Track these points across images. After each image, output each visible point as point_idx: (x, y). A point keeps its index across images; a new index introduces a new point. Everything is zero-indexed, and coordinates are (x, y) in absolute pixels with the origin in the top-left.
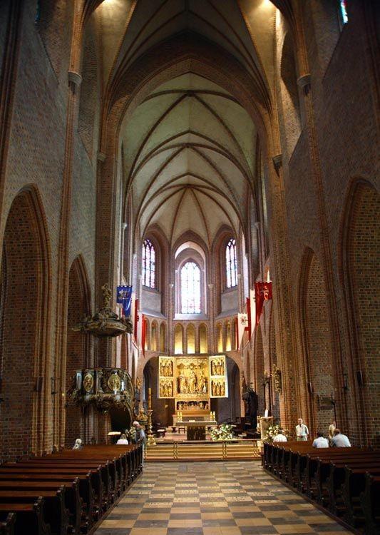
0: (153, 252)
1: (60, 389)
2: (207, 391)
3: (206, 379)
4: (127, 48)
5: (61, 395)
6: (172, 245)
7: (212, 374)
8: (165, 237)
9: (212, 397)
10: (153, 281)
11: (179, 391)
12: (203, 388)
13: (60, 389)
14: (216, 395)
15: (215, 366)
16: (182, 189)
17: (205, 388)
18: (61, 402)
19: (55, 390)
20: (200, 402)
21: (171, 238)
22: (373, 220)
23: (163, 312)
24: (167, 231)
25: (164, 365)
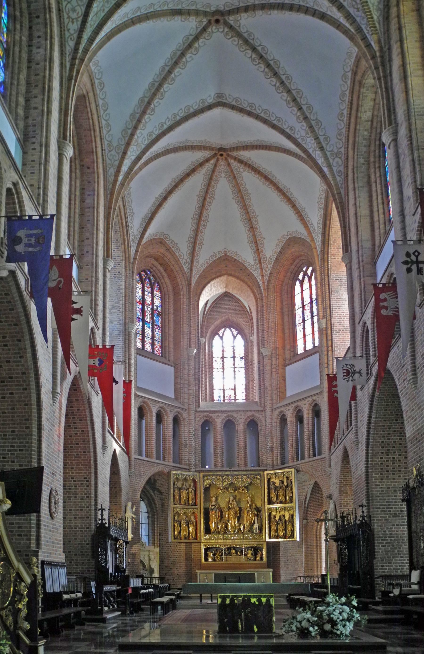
0: (157, 294)
3: (259, 511)
7: (270, 502)
8: (181, 267)
9: (268, 540)
10: (157, 344)
14: (278, 537)
15: (276, 488)
16: (207, 160)
17: (256, 526)
23: (177, 398)
24: (183, 250)
25: (179, 485)
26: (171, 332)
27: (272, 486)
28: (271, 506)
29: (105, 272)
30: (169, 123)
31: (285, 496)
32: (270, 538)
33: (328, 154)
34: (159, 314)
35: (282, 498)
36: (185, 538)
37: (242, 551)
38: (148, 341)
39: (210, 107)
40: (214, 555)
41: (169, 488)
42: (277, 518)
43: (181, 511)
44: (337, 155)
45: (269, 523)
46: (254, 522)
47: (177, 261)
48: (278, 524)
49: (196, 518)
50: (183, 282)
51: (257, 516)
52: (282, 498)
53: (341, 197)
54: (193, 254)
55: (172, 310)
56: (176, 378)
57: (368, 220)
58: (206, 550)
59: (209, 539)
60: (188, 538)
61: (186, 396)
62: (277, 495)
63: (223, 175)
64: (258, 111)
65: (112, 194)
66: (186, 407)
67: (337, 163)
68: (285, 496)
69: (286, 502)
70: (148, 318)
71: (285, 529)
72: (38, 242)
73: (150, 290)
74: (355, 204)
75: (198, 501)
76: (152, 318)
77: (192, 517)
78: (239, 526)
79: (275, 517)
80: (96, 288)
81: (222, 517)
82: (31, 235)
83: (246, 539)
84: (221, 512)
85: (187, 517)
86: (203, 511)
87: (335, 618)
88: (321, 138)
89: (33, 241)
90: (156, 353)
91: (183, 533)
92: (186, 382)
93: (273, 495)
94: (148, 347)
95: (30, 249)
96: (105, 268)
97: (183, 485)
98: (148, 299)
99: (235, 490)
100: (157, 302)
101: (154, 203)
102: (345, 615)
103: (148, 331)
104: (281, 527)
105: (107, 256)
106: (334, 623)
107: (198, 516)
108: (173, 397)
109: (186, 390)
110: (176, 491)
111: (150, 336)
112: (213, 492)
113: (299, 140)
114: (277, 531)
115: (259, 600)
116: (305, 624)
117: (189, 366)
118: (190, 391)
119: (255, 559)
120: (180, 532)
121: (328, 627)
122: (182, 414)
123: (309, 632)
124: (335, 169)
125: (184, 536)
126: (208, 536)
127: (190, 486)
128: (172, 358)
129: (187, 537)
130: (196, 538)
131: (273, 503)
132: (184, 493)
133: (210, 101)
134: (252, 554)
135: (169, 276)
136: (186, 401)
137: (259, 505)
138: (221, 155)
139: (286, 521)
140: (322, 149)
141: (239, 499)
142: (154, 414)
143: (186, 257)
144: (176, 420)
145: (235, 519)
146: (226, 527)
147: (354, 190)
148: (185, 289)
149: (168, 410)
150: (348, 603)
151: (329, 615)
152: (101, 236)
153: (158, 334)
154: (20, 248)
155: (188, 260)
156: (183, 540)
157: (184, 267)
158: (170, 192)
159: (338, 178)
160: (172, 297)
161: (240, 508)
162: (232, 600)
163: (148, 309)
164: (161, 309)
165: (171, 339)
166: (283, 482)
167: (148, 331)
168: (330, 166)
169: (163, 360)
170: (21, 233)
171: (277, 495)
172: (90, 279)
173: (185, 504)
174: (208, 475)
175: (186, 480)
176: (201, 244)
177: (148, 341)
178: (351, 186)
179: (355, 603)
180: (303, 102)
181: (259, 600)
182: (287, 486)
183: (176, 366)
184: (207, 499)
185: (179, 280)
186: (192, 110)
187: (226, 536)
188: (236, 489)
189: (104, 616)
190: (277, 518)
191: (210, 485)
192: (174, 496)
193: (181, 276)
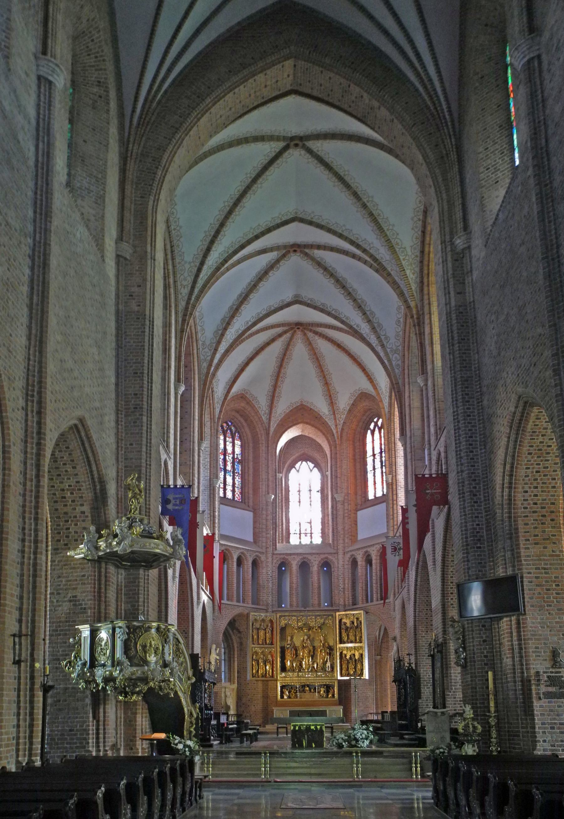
0: (238, 443)
1: (32, 655)
3: (331, 650)
5: (32, 667)
6: (272, 429)
7: (341, 642)
9: (339, 678)
11: (284, 669)
12: (325, 663)
13: (32, 655)
15: (347, 629)
16: (285, 332)
17: (328, 664)
18: (32, 678)
19: (20, 655)
20: (321, 686)
21: (270, 419)
23: (255, 542)
24: (262, 403)
26: (251, 478)
27: (343, 627)
28: (342, 645)
29: (199, 452)
30: (253, 321)
31: (355, 636)
32: (341, 676)
33: (388, 350)
34: (240, 462)
35: (352, 638)
36: (263, 676)
38: (229, 488)
39: (288, 305)
40: (289, 692)
41: (247, 628)
42: (348, 657)
43: (260, 651)
44: (396, 352)
46: (327, 661)
47: (257, 412)
48: (348, 663)
49: (272, 656)
50: (262, 432)
52: (352, 638)
53: (399, 387)
54: (271, 406)
55: (251, 458)
56: (255, 522)
57: (420, 411)
58: (282, 687)
59: (285, 677)
60: (265, 676)
61: (264, 539)
62: (348, 635)
63: (300, 341)
64: (329, 309)
65: (205, 384)
66: (264, 551)
67: (396, 358)
68: (355, 636)
69: (355, 642)
70: (229, 468)
71: (355, 668)
72: (181, 503)
73: (231, 440)
74: (410, 397)
75: (275, 640)
76: (233, 467)
77: (269, 656)
78: (313, 664)
79: (346, 656)
80: (193, 470)
81: (297, 656)
82: (177, 498)
83: (319, 676)
84: (296, 650)
85: (264, 655)
86: (279, 650)
87: (357, 737)
88: (383, 338)
89: (178, 503)
90: (236, 499)
91: (260, 672)
92: (264, 527)
93: (344, 635)
94: (229, 495)
95: (177, 508)
96: (199, 449)
97: (261, 625)
98: (229, 449)
99: (309, 630)
100: (238, 450)
101: (237, 369)
102: (364, 736)
103: (229, 480)
104: (351, 666)
105: (201, 439)
106: (357, 740)
107: (275, 655)
108: (252, 540)
109: (264, 534)
110: (255, 631)
111: (231, 484)
112: (288, 631)
113: (365, 335)
114: (348, 669)
116: (340, 741)
117: (267, 511)
118: (268, 535)
119: (327, 697)
120: (258, 671)
121: (354, 743)
122: (260, 558)
123: (343, 746)
124: (394, 363)
125: (262, 674)
126: (283, 674)
127: (267, 626)
128: (251, 504)
129: (264, 675)
130: (273, 676)
131: (344, 643)
132: (262, 633)
133: (289, 300)
135: (249, 426)
136: (264, 544)
137: (331, 644)
138: (298, 328)
139: (356, 660)
140: (383, 346)
141: (313, 638)
142: (235, 560)
143: (264, 409)
144: (255, 563)
145: (308, 657)
146: (301, 665)
147: (409, 384)
148: (263, 438)
149: (248, 555)
150: (367, 729)
151: (354, 736)
152: (196, 423)
153: (238, 480)
154: (170, 507)
155: (267, 411)
156: (260, 678)
157: (263, 418)
158: (251, 359)
159: (397, 371)
160: (251, 445)
161: (314, 647)
162: (300, 727)
163: (229, 458)
164: (242, 457)
165: (251, 486)
166: (353, 623)
167: (229, 480)
168: (389, 360)
169: (243, 505)
170: (170, 497)
171: (348, 635)
172: (188, 463)
173: (263, 644)
174: (284, 616)
175: (263, 620)
176: (279, 397)
177: (229, 488)
178: (406, 380)
179: (371, 729)
180: (367, 309)
182: (357, 627)
183: (255, 511)
184: (283, 637)
185: (258, 430)
186: (273, 308)
187: (300, 674)
188: (310, 628)
189: (212, 742)
190: (348, 657)
191: (286, 625)
192: (253, 636)
193: (260, 426)
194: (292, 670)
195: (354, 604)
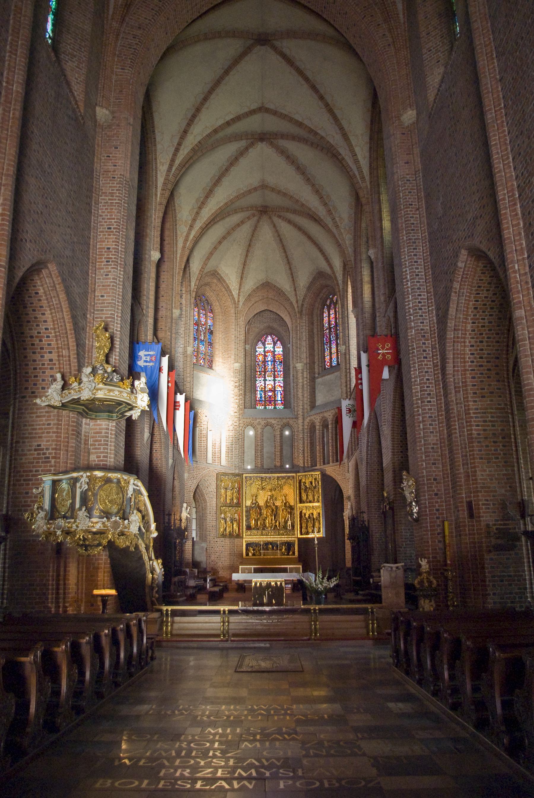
2: (293, 526)
4: (159, 239)
7: (301, 501)
9: (299, 536)
11: (249, 528)
12: (286, 522)
17: (289, 523)
22: (467, 340)
27: (303, 487)
32: (301, 534)
37: (277, 546)
42: (307, 516)
45: (300, 521)
51: (290, 513)
52: (311, 498)
58: (248, 545)
62: (307, 496)
78: (276, 522)
79: (305, 515)
84: (261, 510)
114: (307, 528)
115: (276, 584)
126: (249, 533)
131: (304, 503)
134: (286, 549)
139: (314, 519)
145: (271, 516)
162: (261, 584)
166: (311, 483)
181: (276, 584)
182: (315, 487)
187: (264, 532)
190: (307, 516)
194: (257, 528)
195: (312, 467)
